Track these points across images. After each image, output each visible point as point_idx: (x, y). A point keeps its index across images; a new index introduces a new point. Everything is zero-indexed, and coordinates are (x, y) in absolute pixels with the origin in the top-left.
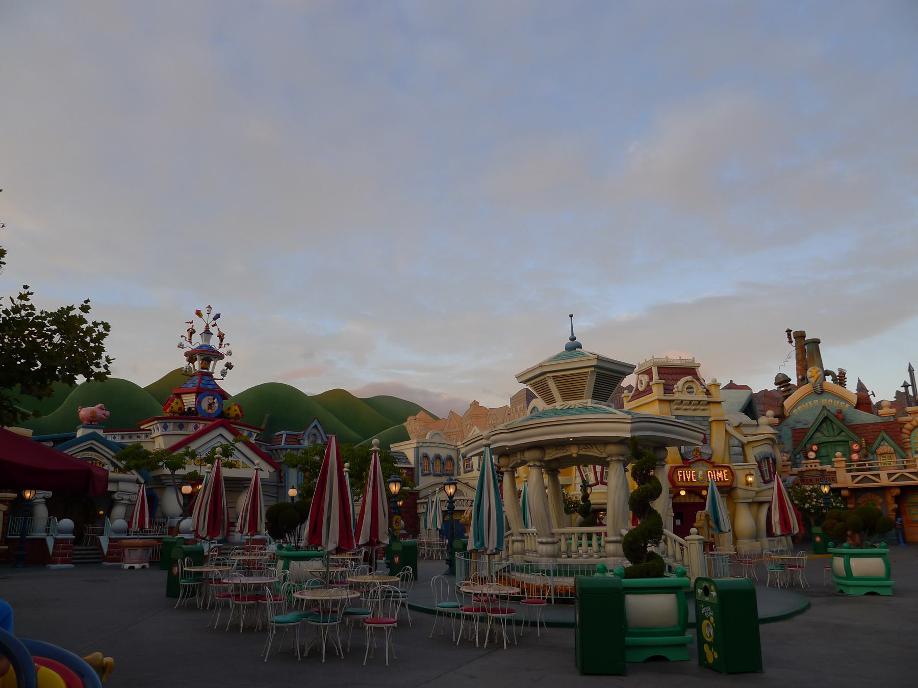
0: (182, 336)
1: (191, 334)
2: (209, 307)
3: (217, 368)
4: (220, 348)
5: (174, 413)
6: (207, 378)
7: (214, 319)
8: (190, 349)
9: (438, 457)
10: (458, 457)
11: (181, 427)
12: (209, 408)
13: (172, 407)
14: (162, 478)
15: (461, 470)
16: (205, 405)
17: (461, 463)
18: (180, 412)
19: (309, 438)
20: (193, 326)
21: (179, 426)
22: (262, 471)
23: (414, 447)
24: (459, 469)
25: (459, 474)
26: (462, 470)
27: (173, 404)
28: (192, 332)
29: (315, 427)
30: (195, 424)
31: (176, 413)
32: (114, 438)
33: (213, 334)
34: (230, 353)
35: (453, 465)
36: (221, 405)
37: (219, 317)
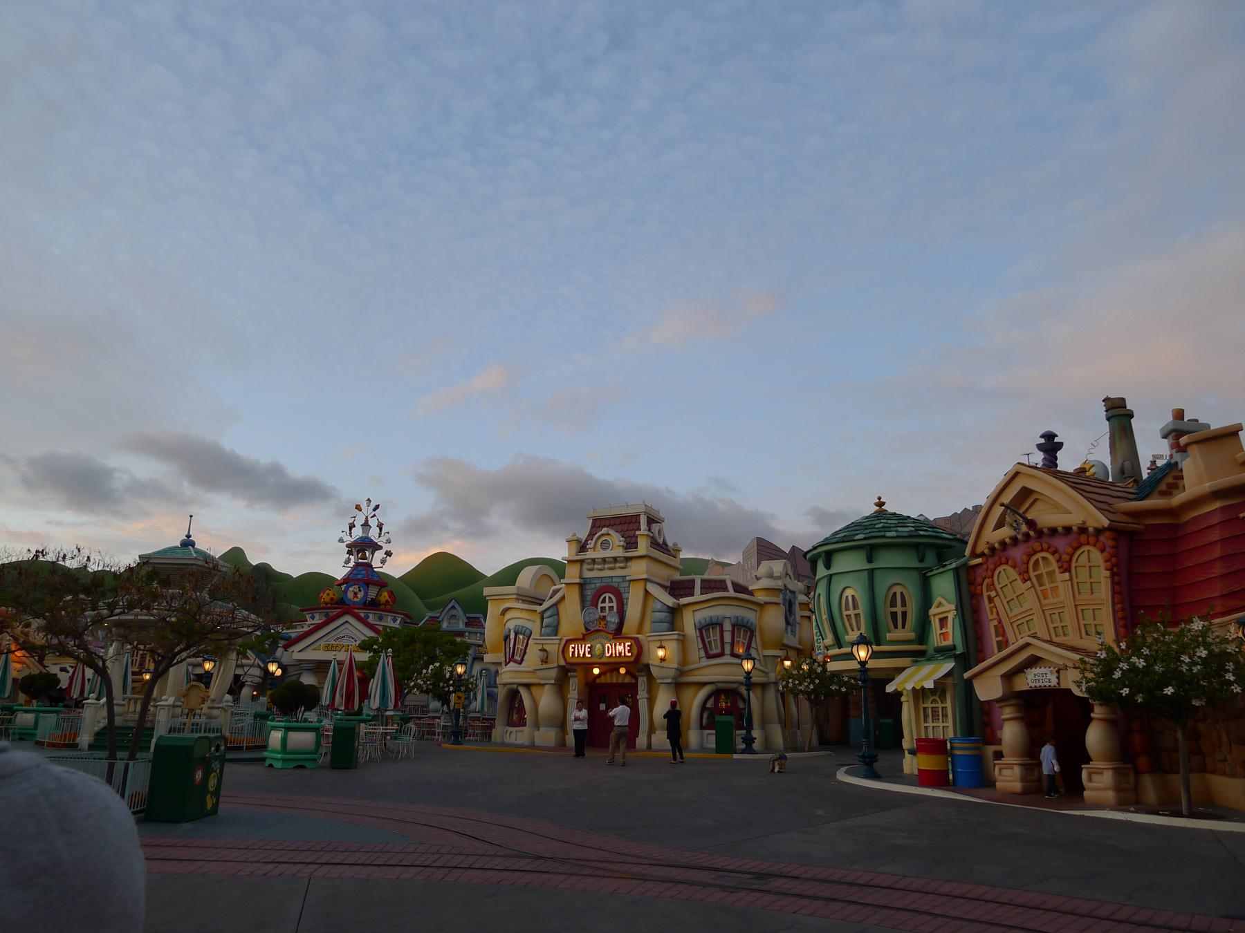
0: (343, 532)
3: (376, 560)
5: (326, 603)
7: (374, 510)
16: (350, 595)
28: (352, 526)
29: (453, 607)
34: (389, 541)
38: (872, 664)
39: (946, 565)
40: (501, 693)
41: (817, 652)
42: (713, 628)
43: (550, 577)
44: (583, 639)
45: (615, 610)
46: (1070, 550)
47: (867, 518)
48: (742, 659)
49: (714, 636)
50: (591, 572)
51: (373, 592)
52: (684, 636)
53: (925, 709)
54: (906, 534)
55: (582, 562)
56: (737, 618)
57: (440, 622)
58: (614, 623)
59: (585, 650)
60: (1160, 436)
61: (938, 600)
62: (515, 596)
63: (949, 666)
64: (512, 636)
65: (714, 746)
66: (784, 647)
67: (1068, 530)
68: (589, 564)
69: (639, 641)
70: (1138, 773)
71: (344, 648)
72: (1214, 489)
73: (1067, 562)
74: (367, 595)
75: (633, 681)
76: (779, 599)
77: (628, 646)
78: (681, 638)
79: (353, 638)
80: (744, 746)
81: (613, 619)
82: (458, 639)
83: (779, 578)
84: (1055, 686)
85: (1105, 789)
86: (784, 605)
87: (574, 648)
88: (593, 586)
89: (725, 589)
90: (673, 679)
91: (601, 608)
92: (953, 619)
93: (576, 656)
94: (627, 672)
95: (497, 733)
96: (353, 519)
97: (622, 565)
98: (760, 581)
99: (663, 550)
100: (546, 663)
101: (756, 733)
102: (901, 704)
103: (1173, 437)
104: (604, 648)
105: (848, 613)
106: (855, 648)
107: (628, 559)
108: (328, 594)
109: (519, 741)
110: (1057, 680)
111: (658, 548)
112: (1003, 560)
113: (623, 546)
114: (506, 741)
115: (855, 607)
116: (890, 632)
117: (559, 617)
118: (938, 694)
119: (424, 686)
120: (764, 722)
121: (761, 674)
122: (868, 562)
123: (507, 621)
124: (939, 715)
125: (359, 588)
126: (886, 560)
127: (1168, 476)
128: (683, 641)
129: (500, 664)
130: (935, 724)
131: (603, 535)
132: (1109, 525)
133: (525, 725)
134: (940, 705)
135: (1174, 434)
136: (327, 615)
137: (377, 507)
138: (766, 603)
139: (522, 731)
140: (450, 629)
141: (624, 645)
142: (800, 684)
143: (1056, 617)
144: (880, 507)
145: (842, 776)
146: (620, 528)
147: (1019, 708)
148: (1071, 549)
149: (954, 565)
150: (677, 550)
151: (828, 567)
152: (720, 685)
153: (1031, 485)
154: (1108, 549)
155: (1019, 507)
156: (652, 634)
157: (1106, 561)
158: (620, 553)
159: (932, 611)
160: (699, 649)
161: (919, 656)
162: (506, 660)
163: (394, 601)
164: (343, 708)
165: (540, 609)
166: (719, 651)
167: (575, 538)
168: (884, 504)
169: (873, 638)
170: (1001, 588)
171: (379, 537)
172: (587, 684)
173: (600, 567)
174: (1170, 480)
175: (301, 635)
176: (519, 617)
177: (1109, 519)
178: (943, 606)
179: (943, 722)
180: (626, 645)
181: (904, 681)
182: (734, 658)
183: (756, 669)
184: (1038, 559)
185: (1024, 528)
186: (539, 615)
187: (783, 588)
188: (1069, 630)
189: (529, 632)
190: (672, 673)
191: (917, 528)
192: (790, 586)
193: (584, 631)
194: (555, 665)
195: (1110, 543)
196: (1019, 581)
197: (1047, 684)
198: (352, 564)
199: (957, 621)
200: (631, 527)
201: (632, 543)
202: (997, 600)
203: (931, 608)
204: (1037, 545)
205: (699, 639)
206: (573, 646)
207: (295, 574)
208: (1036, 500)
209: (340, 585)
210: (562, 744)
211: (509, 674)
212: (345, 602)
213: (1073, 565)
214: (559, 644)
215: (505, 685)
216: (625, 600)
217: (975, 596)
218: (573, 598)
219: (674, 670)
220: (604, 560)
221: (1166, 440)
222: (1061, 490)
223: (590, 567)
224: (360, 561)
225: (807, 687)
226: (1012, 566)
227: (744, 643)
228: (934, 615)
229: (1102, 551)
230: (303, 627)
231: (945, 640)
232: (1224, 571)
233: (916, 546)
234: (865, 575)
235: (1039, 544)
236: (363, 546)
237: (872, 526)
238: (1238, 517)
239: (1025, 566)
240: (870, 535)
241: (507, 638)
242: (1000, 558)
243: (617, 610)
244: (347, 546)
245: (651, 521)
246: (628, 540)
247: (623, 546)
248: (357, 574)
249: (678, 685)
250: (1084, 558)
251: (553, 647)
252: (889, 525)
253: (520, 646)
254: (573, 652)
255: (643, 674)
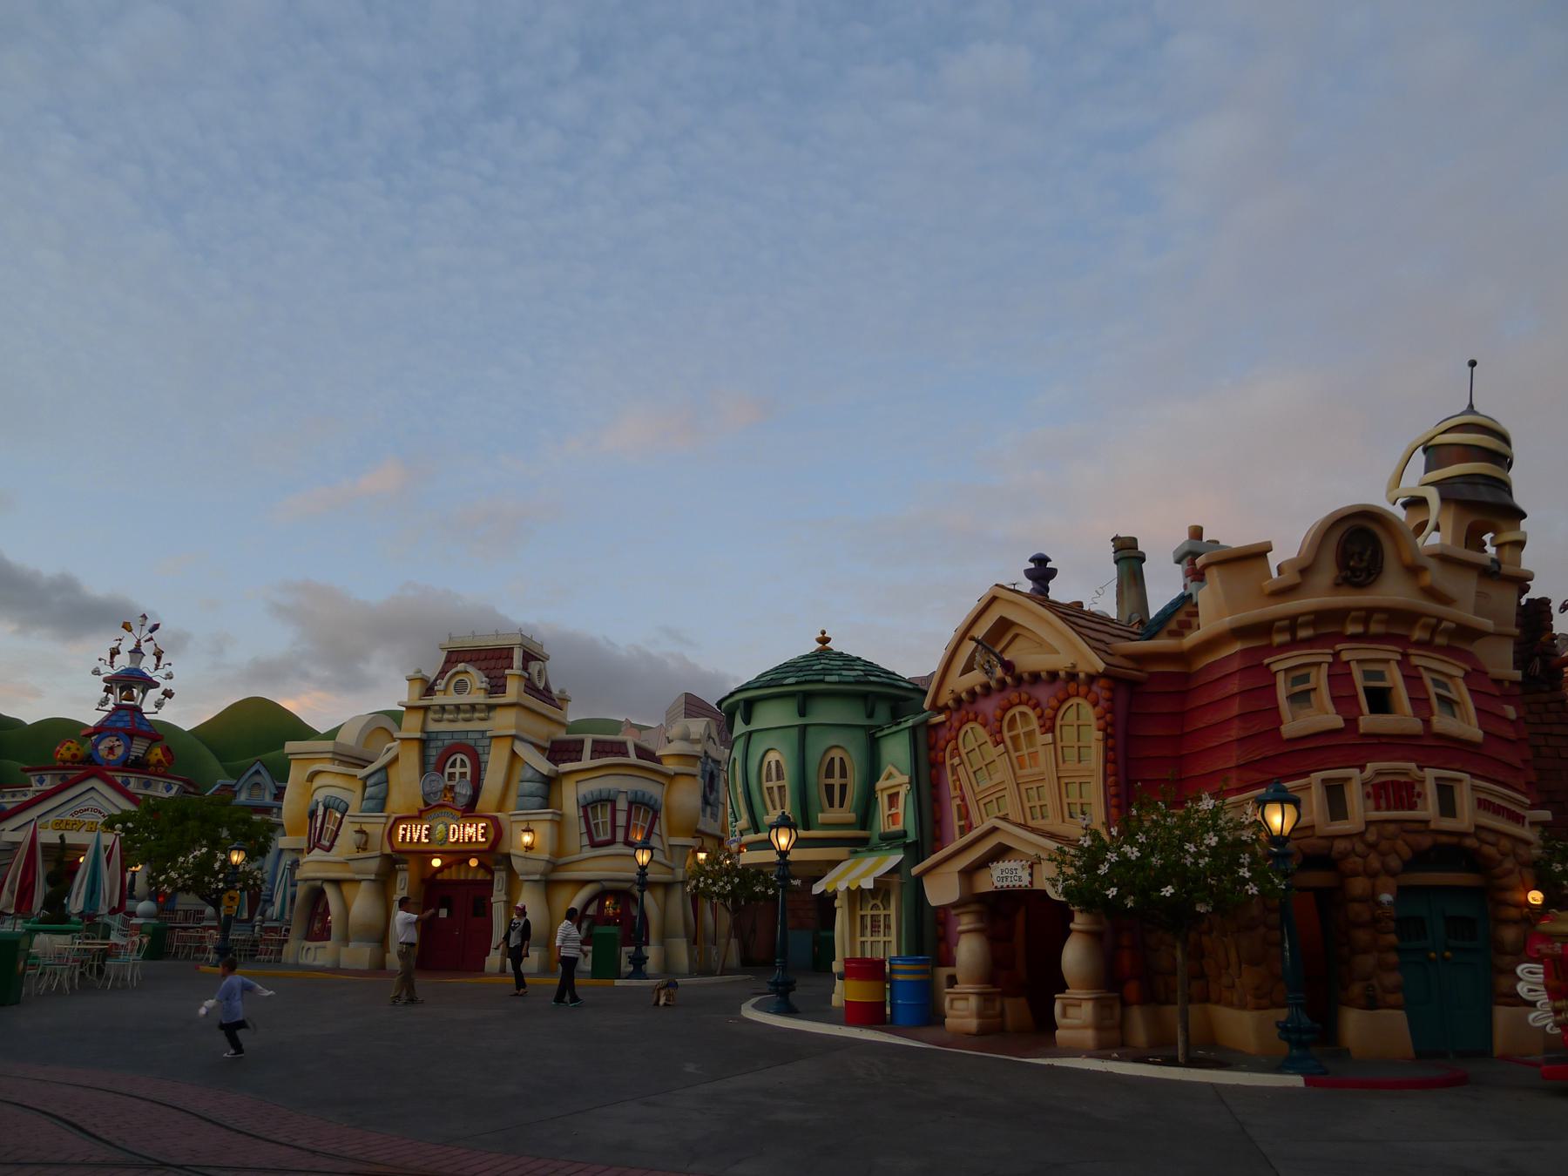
0: (100, 660)
5: (65, 761)
28: (115, 652)
29: (257, 772)
34: (169, 676)
38: (795, 855)
39: (900, 723)
40: (301, 891)
41: (731, 839)
42: (602, 806)
43: (386, 729)
44: (419, 817)
45: (468, 778)
46: (1054, 703)
47: (804, 657)
48: (636, 849)
49: (603, 817)
50: (436, 723)
51: (138, 748)
52: (561, 815)
53: (862, 917)
54: (852, 679)
55: (426, 709)
56: (636, 793)
57: (236, 792)
58: (465, 795)
59: (420, 833)
60: (1172, 560)
61: (888, 769)
62: (330, 756)
63: (895, 858)
64: (320, 812)
65: (590, 968)
66: (699, 834)
67: (1054, 675)
68: (435, 712)
69: (498, 823)
70: (1125, 1004)
71: (85, 828)
72: (1234, 626)
73: (1050, 719)
74: (130, 751)
75: (489, 878)
76: (697, 769)
77: (482, 828)
78: (557, 818)
79: (100, 813)
80: (631, 968)
81: (464, 790)
82: (256, 818)
83: (698, 741)
84: (1026, 886)
85: (1085, 1027)
86: (703, 777)
87: (405, 829)
88: (440, 743)
89: (626, 754)
90: (542, 874)
91: (449, 774)
92: (906, 795)
93: (408, 840)
94: (480, 865)
95: (289, 950)
96: (119, 642)
97: (482, 715)
98: (672, 744)
99: (543, 698)
100: (365, 849)
101: (652, 952)
102: (834, 910)
103: (1188, 562)
104: (448, 830)
105: (770, 784)
106: (774, 832)
107: (491, 708)
108: (69, 749)
109: (319, 962)
110: (1029, 879)
111: (536, 695)
112: (971, 715)
113: (485, 690)
114: (301, 961)
115: (779, 776)
116: (823, 811)
117: (388, 785)
118: (880, 898)
119: (180, 881)
120: (665, 936)
121: (664, 869)
122: (800, 716)
123: (315, 790)
124: (880, 926)
126: (825, 713)
127: (1183, 610)
128: (559, 823)
129: (301, 851)
130: (873, 939)
131: (458, 673)
132: (1105, 669)
133: (329, 939)
134: (882, 912)
135: (1189, 557)
136: (63, 777)
137: (156, 627)
138: (676, 774)
139: (324, 947)
140: (248, 803)
141: (477, 826)
142: (714, 884)
143: (1033, 793)
144: (824, 644)
145: (749, 1012)
146: (484, 664)
147: (980, 916)
148: (1056, 701)
149: (910, 723)
150: (564, 700)
151: (747, 721)
152: (608, 885)
153: (1012, 615)
154: (1102, 702)
155: (995, 643)
156: (517, 812)
157: (1098, 719)
158: (479, 698)
159: (881, 784)
160: (581, 834)
161: (859, 845)
162: (309, 845)
163: (169, 762)
164: (12, 911)
165: (361, 773)
166: (608, 837)
167: (419, 675)
168: (828, 640)
169: (801, 819)
170: (967, 753)
171: (156, 668)
172: (423, 881)
173: (451, 717)
174: (1181, 616)
175: (17, 807)
176: (333, 785)
177: (1104, 662)
178: (895, 777)
179: (885, 936)
180: (479, 828)
181: (836, 880)
182: (628, 848)
183: (655, 862)
184: (1015, 715)
185: (999, 672)
186: (361, 783)
187: (702, 755)
188: (1050, 811)
189: (345, 807)
190: (541, 866)
191: (867, 672)
192: (713, 753)
193: (422, 807)
194: (377, 853)
195: (1105, 694)
196: (990, 744)
197: (1017, 884)
198: (110, 706)
199: (910, 799)
200: (500, 663)
201: (500, 686)
202: (961, 770)
203: (878, 780)
204: (1014, 696)
205: (582, 820)
206: (405, 826)
207: (29, 720)
208: (1016, 636)
209: (89, 735)
210: (380, 966)
211: (314, 865)
212: (93, 760)
213: (1058, 723)
214: (385, 824)
215: (306, 880)
216: (483, 765)
217: (936, 765)
218: (411, 758)
219: (543, 864)
220: (457, 708)
221: (1179, 566)
222: (1049, 623)
223: (437, 716)
224: (124, 702)
225: (723, 887)
226: (981, 724)
227: (643, 828)
228: (882, 790)
229: (1095, 705)
230: (25, 795)
231: (894, 824)
232: (1243, 734)
233: (864, 696)
234: (794, 733)
235: (1017, 694)
236: (130, 682)
237: (808, 668)
238: (1262, 664)
239: (998, 724)
240: (803, 679)
241: (313, 814)
242: (968, 713)
243: (471, 777)
244: (105, 680)
245: (529, 657)
246: (494, 682)
247: (485, 690)
248: (116, 721)
249: (549, 884)
250: (1071, 714)
251: (376, 828)
252: (830, 667)
253: (331, 827)
254: (404, 836)
255: (502, 867)
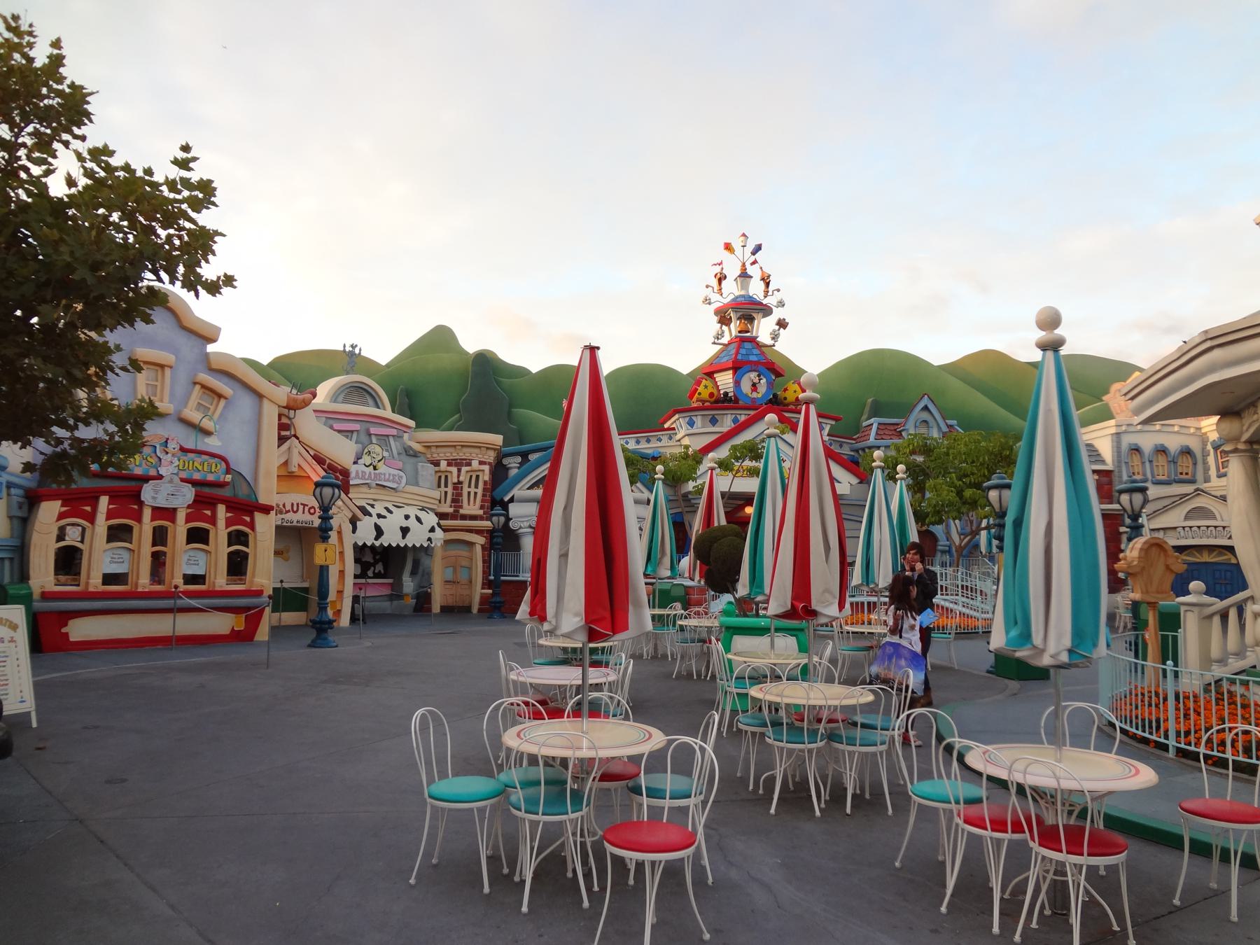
0: (707, 287)
1: (720, 281)
2: (744, 235)
3: (763, 329)
4: (765, 297)
5: (703, 401)
6: (748, 345)
7: (754, 253)
8: (722, 304)
9: (1161, 450)
10: (1204, 449)
11: (714, 421)
12: (753, 391)
13: (700, 394)
14: (690, 497)
15: (1210, 473)
16: (746, 387)
17: (1211, 460)
18: (713, 400)
19: (916, 427)
20: (722, 269)
21: (710, 421)
22: (840, 483)
23: (1112, 434)
24: (1207, 469)
25: (1207, 480)
26: (1213, 472)
27: (701, 389)
28: (721, 278)
29: (926, 408)
30: (734, 416)
31: (707, 401)
32: (627, 443)
33: (752, 277)
34: (781, 304)
35: (1195, 464)
36: (770, 385)
37: (761, 249)
108: (706, 387)
125: (759, 376)
137: (758, 248)
